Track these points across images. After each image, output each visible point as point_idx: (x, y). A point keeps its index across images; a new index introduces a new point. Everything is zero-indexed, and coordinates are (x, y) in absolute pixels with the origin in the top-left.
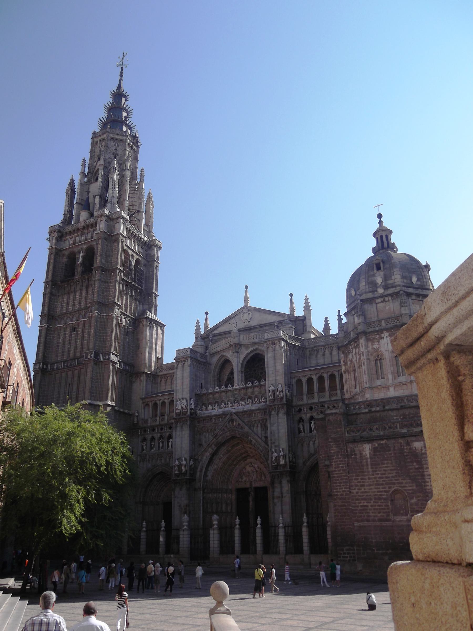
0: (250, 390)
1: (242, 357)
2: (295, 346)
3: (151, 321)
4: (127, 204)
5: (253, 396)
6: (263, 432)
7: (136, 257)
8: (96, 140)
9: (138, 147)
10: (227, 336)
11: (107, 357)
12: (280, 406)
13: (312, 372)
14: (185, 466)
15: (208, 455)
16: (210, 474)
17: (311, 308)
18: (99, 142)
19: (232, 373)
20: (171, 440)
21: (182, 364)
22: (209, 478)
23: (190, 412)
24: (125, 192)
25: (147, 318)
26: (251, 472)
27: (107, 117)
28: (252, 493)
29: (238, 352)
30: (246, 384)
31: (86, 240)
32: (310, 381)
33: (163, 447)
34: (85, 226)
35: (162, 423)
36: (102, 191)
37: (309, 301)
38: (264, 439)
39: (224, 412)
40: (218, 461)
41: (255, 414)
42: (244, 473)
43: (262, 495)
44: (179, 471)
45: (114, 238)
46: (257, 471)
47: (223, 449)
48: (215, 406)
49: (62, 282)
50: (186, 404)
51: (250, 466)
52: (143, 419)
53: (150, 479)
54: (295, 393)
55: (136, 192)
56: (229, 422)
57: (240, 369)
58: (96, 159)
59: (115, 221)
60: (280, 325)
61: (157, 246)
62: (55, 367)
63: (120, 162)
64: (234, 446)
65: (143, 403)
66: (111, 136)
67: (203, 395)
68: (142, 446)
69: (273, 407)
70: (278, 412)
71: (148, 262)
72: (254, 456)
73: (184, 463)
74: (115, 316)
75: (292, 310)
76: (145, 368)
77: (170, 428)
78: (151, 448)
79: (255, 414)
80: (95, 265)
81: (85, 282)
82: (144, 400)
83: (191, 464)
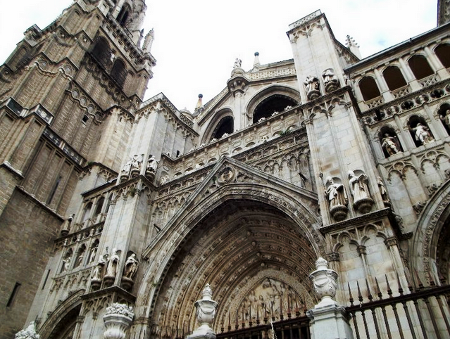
14: (115, 262)
15: (169, 247)
17: (358, 45)
23: (146, 173)
26: (265, 298)
40: (194, 268)
44: (99, 276)
47: (206, 242)
52: (77, 224)
53: (60, 319)
56: (221, 173)
57: (244, 111)
61: (150, 59)
64: (229, 233)
68: (64, 263)
69: (318, 105)
70: (331, 108)
71: (137, 72)
73: (114, 257)
78: (77, 264)
82: (86, 198)
83: (128, 261)
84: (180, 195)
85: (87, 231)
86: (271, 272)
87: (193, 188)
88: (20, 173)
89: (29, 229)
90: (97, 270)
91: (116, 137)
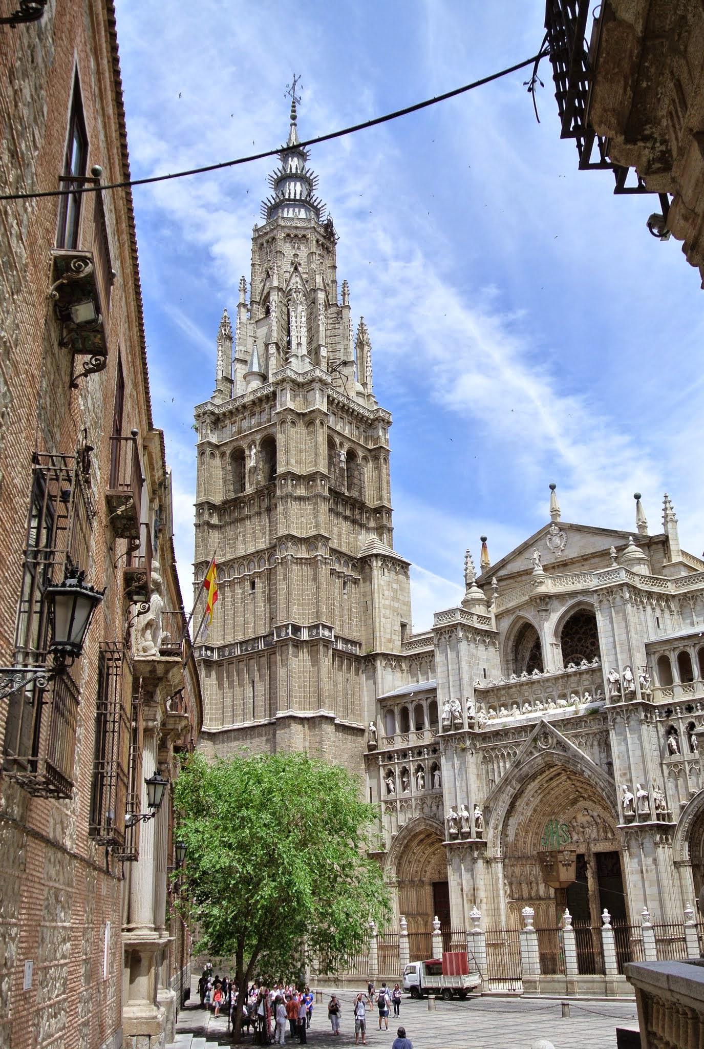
0: (573, 679)
1: (555, 617)
2: (650, 595)
3: (384, 558)
4: (323, 352)
5: (581, 689)
6: (604, 755)
7: (347, 446)
8: (260, 241)
9: (334, 243)
10: (524, 578)
11: (314, 632)
12: (631, 708)
13: (686, 642)
16: (511, 831)
17: (676, 517)
18: (265, 245)
19: (538, 646)
20: (437, 773)
21: (447, 637)
22: (511, 838)
24: (318, 332)
25: (377, 556)
27: (274, 196)
28: (592, 864)
29: (547, 610)
30: (566, 667)
31: (259, 424)
32: (684, 660)
33: (423, 787)
34: (257, 401)
35: (421, 743)
36: (278, 333)
37: (672, 505)
38: (605, 767)
39: (529, 720)
41: (586, 722)
42: (574, 827)
43: (610, 868)
45: (307, 418)
46: (597, 823)
47: (533, 786)
48: (512, 709)
49: (225, 503)
50: (459, 709)
51: (583, 815)
54: (657, 684)
55: (337, 326)
58: (264, 275)
59: (306, 388)
60: (620, 554)
61: (383, 420)
62: (227, 653)
63: (305, 276)
64: (551, 779)
65: (383, 707)
66: (288, 231)
67: (488, 691)
68: (388, 785)
70: (628, 718)
72: (590, 796)
73: (465, 814)
74: (319, 558)
75: (642, 526)
76: (381, 646)
77: (435, 751)
79: (586, 722)
80: (280, 470)
81: (263, 500)
83: (477, 816)
84: (505, 748)
85: (404, 754)
86: (588, 804)
87: (517, 744)
88: (332, 715)
89: (346, 756)
90: (452, 823)
91: (387, 602)
